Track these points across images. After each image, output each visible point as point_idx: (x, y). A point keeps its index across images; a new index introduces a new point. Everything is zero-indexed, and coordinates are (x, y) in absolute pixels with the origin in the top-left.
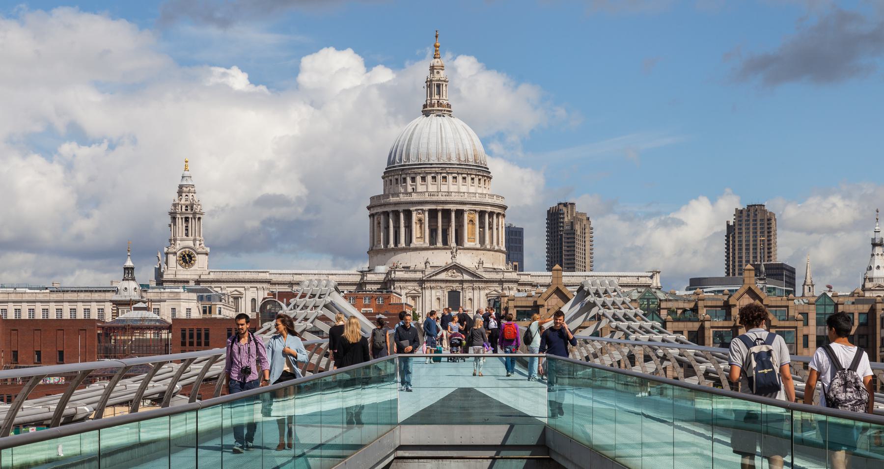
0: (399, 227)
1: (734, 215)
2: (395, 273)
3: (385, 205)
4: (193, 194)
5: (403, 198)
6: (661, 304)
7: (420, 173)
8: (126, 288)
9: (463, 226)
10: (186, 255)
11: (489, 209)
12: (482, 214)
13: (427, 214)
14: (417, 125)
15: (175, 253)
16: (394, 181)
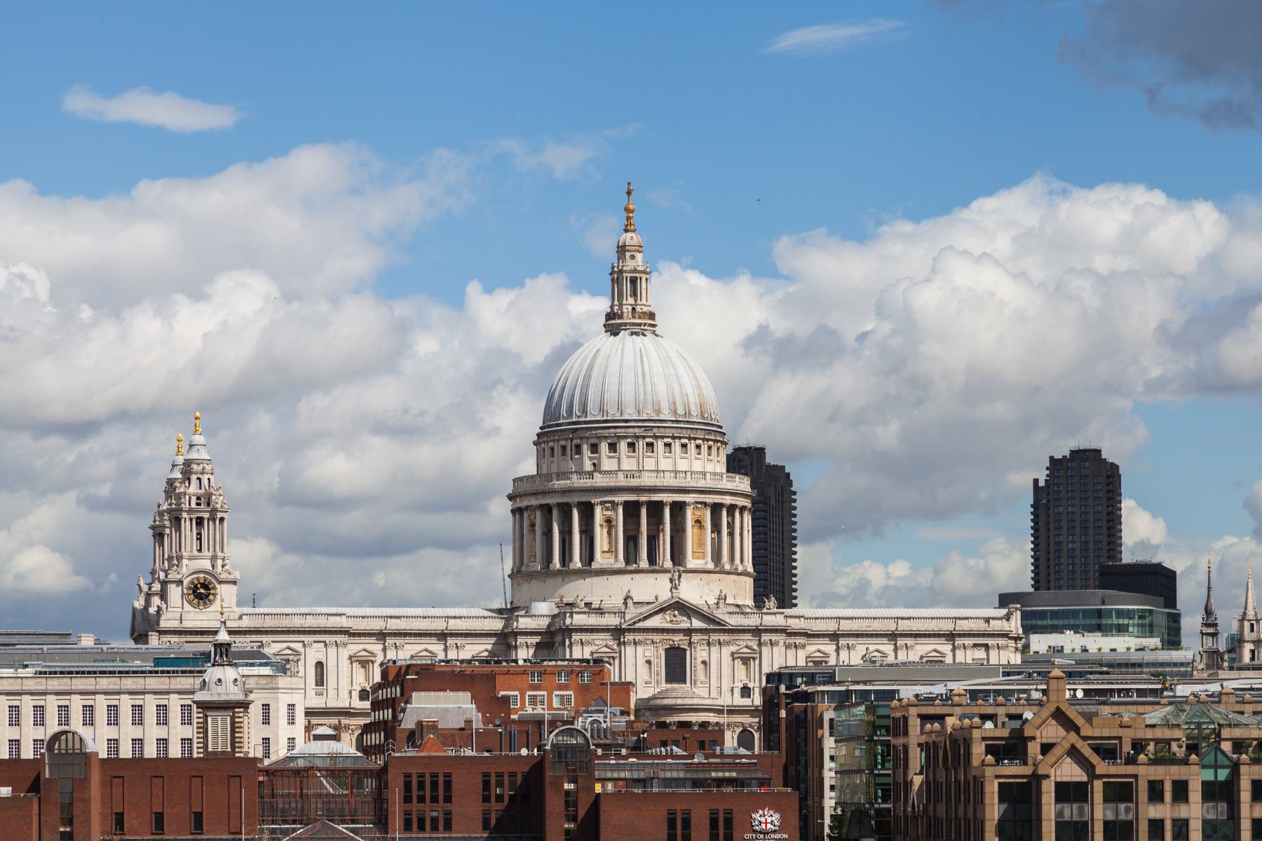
0: (570, 532)
1: (1047, 469)
2: (571, 617)
3: (544, 493)
4: (210, 476)
5: (576, 481)
6: (1222, 731)
7: (606, 438)
8: (220, 680)
9: (684, 530)
10: (199, 586)
11: (728, 500)
12: (716, 509)
13: (620, 510)
14: (598, 351)
15: (180, 582)
16: (557, 451)
